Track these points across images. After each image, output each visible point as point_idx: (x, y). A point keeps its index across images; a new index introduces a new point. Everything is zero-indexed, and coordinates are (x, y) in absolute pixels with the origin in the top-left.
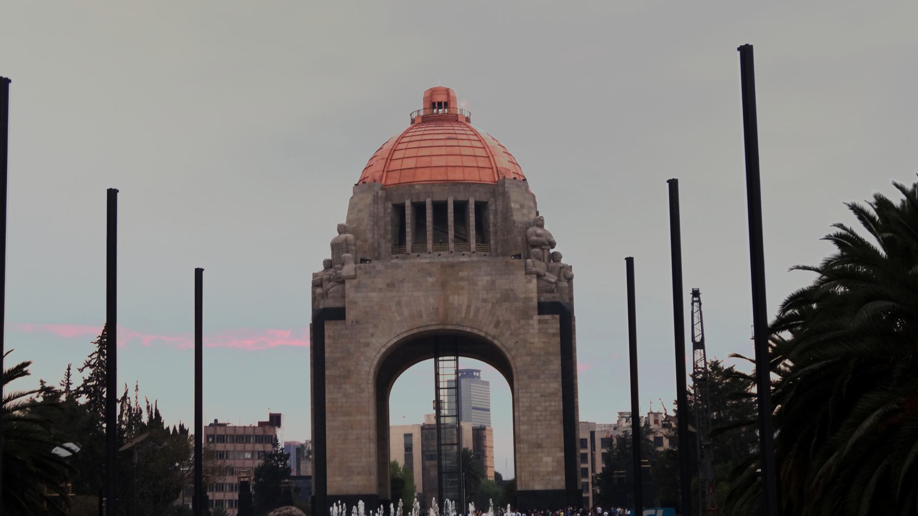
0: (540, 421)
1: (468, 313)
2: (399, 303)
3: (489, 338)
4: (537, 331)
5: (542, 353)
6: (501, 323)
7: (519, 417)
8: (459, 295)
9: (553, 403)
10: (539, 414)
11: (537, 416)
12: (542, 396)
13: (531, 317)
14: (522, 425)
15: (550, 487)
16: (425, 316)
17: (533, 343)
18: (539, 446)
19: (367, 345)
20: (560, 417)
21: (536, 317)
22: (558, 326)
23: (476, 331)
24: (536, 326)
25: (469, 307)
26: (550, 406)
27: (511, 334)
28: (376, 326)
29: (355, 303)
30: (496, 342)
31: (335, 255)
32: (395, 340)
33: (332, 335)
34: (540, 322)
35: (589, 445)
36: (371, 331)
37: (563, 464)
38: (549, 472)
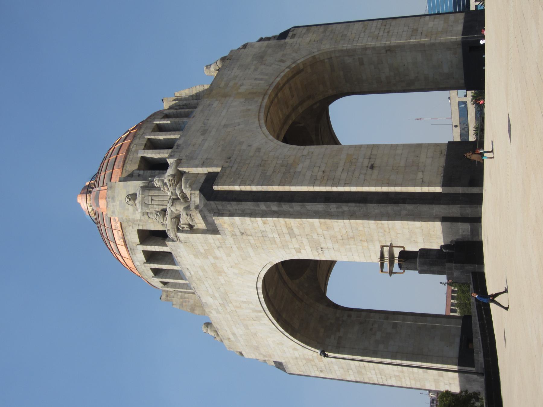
1: (261, 79)
2: (226, 126)
3: (293, 65)
4: (301, 39)
8: (241, 86)
12: (364, 32)
13: (286, 43)
16: (250, 107)
19: (258, 150)
21: (287, 40)
23: (282, 74)
24: (295, 40)
25: (256, 79)
27: (296, 52)
28: (241, 143)
29: (207, 159)
30: (299, 62)
31: (154, 203)
32: (265, 129)
33: (232, 179)
36: (244, 147)
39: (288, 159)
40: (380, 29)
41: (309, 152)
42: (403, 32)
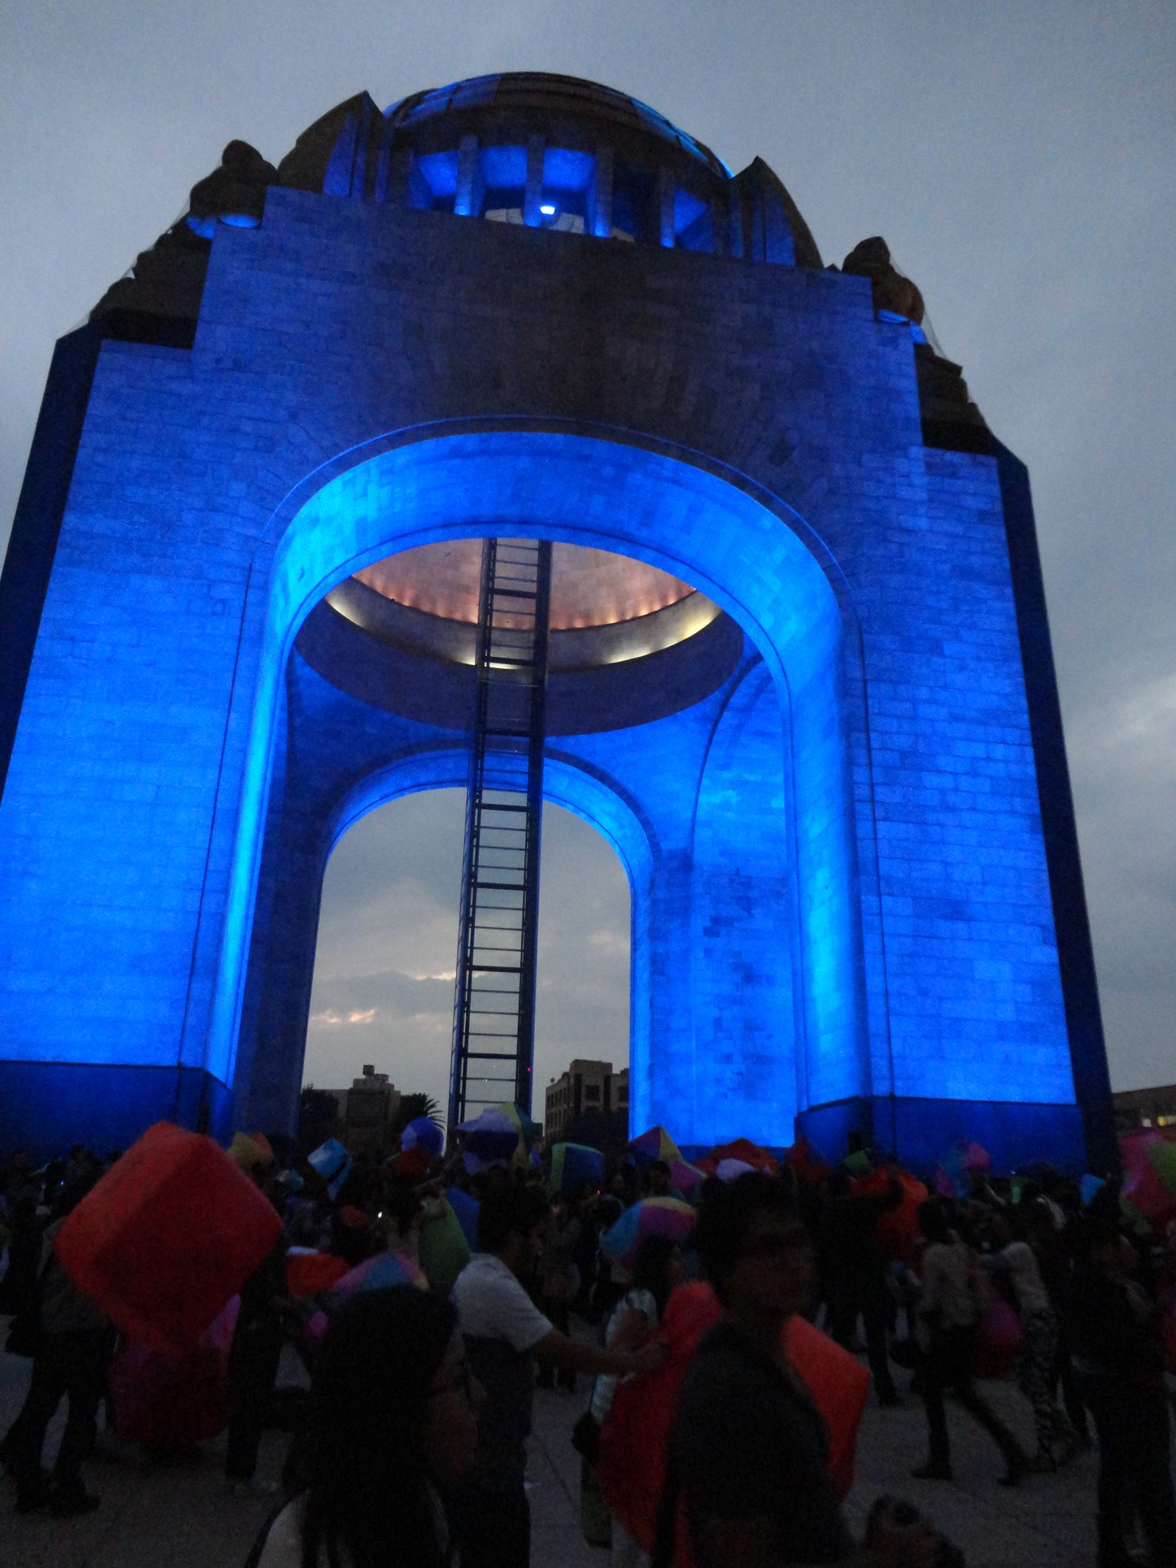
0: (953, 809)
4: (922, 495)
5: (946, 568)
6: (793, 448)
7: (872, 786)
9: (999, 751)
10: (948, 782)
11: (943, 792)
12: (954, 718)
13: (902, 449)
14: (885, 819)
15: (1013, 1094)
17: (910, 531)
18: (956, 911)
20: (1029, 803)
21: (918, 451)
22: (996, 489)
24: (920, 479)
26: (989, 759)
34: (929, 466)
35: (601, 1095)
37: (1058, 994)
38: (1001, 1025)
39: (198, 544)
40: (974, 774)
41: (223, 602)
42: (946, 864)
